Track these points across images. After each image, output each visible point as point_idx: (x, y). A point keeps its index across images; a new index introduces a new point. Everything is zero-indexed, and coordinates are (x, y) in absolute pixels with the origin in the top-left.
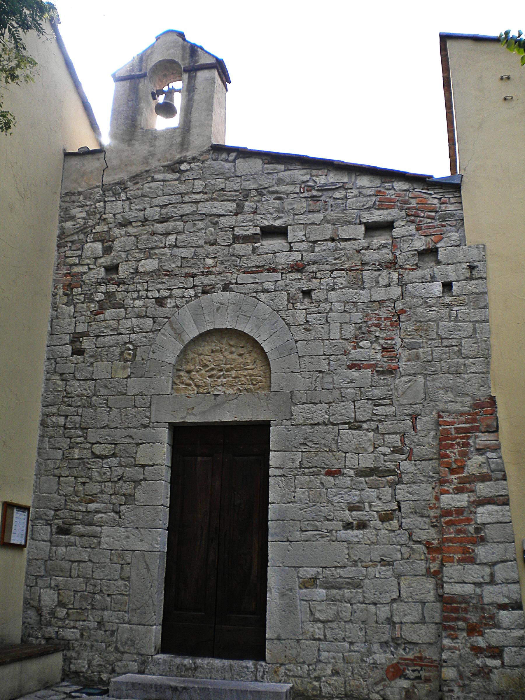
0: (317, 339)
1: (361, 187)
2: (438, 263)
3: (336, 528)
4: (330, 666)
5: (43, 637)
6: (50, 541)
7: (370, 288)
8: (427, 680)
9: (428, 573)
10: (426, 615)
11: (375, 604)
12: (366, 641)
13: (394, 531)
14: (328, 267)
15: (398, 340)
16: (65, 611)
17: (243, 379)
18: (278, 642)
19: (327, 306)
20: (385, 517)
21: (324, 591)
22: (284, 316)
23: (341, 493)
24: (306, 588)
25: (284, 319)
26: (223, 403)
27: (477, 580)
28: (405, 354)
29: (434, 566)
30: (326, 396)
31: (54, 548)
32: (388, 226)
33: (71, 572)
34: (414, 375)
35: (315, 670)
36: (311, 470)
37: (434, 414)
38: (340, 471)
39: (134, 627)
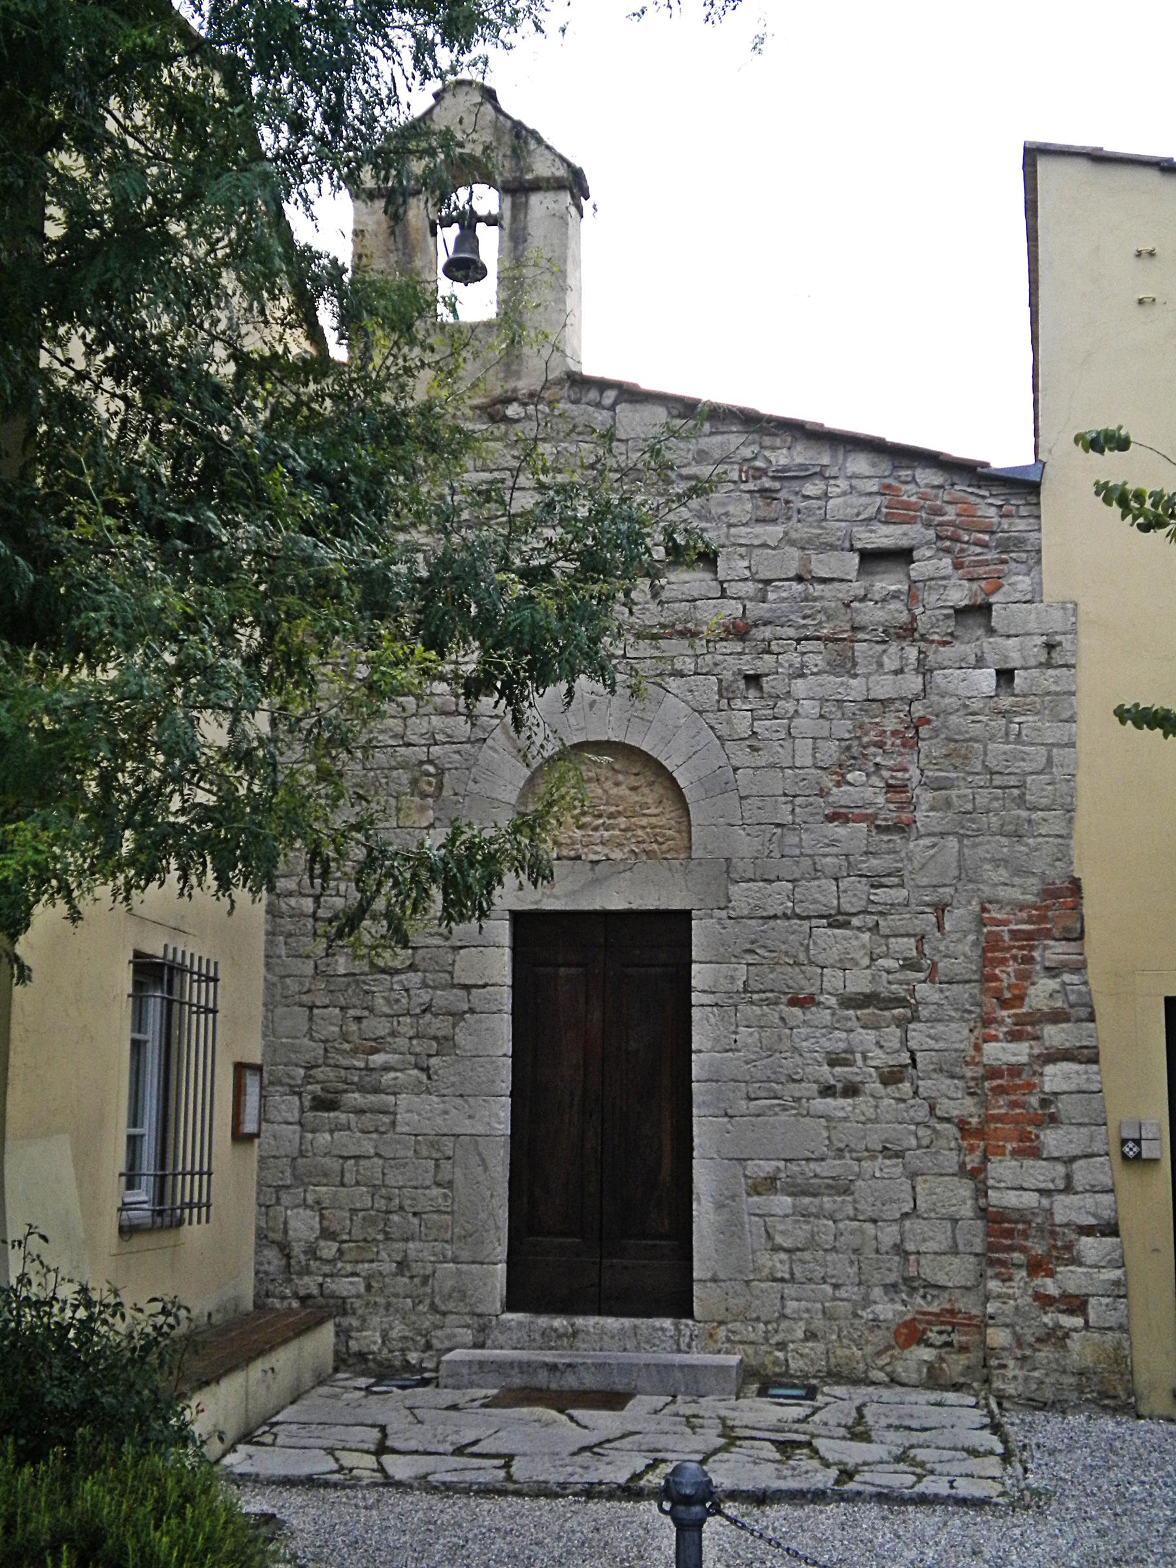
0: (773, 766)
1: (854, 476)
2: (991, 631)
3: (807, 1094)
4: (801, 1323)
5: (296, 1295)
6: (300, 1123)
7: (867, 676)
8: (963, 1349)
9: (963, 1171)
10: (960, 1242)
11: (875, 1221)
12: (860, 1284)
13: (904, 1101)
14: (791, 632)
15: (914, 772)
16: (335, 1246)
17: (640, 832)
18: (713, 1285)
19: (790, 706)
20: (890, 1077)
21: (789, 1199)
22: (713, 722)
23: (814, 1036)
24: (759, 1194)
25: (712, 728)
26: (606, 878)
27: (1042, 1186)
28: (926, 797)
29: (972, 1161)
30: (788, 868)
31: (310, 1136)
32: (904, 556)
33: (343, 1176)
34: (942, 835)
35: (776, 1331)
36: (763, 996)
37: (975, 906)
38: (813, 999)
39: (464, 1267)
